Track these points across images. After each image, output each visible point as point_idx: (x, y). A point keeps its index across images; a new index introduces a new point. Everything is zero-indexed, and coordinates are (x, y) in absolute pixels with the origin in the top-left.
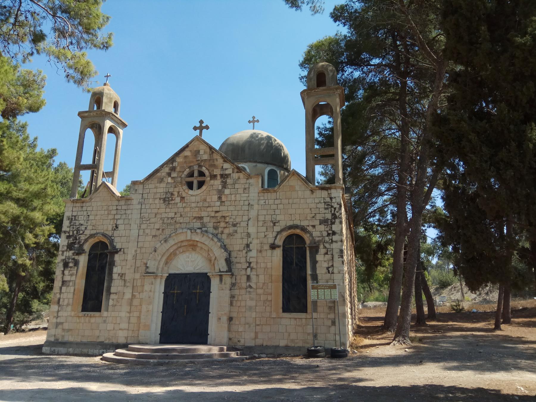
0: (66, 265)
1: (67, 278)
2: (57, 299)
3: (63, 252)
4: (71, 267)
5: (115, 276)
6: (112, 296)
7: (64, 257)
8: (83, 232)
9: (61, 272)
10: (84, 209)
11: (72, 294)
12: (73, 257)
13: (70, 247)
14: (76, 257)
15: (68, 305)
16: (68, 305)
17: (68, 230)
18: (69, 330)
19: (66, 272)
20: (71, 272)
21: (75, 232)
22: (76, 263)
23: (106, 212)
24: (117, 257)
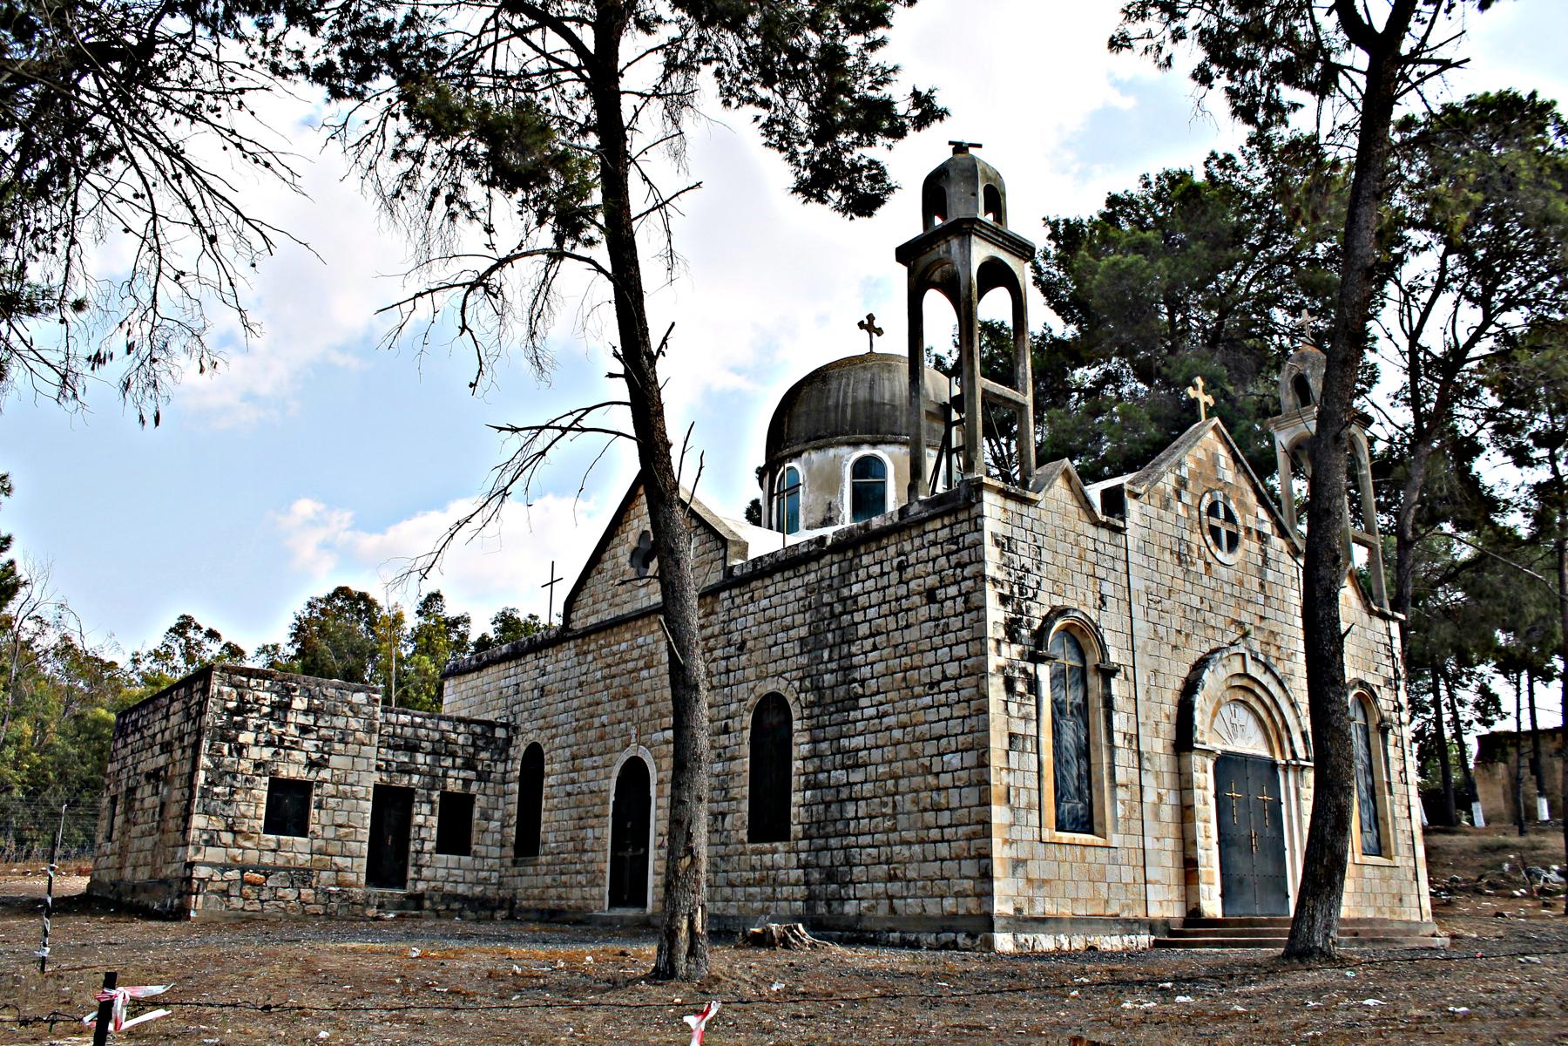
0: (1009, 685)
1: (1018, 727)
2: (1003, 789)
3: (998, 642)
4: (1022, 695)
5: (1118, 739)
6: (1121, 793)
7: (1002, 661)
8: (1035, 595)
9: (1002, 705)
10: (1027, 523)
11: (1036, 776)
12: (1022, 664)
13: (1012, 629)
14: (1030, 668)
15: (1029, 808)
16: (1029, 808)
17: (1000, 576)
18: (1044, 882)
19: (1013, 707)
20: (1023, 710)
21: (1016, 589)
22: (1033, 685)
23: (1076, 551)
24: (1117, 687)
